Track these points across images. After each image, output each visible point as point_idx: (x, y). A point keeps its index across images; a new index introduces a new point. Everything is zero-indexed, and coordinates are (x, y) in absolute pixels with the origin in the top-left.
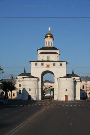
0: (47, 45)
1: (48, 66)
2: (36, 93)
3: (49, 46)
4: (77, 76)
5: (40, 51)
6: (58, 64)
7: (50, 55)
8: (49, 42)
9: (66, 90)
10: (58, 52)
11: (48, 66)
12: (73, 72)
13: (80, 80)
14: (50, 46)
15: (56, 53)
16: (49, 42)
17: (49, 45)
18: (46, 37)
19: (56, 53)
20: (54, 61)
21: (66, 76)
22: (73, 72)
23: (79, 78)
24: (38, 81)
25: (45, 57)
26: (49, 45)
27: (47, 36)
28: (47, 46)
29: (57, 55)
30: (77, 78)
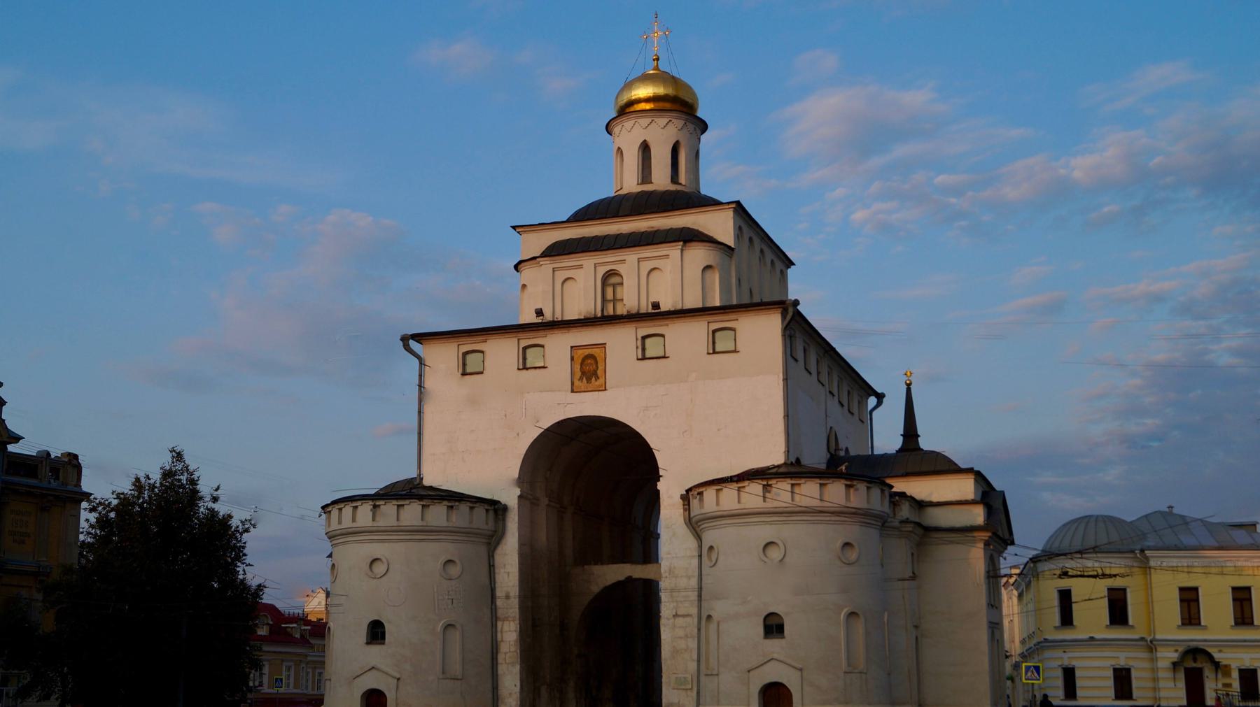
1: (589, 370)
2: (456, 669)
4: (941, 466)
6: (687, 338)
7: (628, 262)
8: (645, 148)
9: (773, 627)
11: (589, 370)
12: (910, 433)
13: (977, 515)
15: (689, 237)
16: (645, 148)
19: (689, 237)
22: (910, 433)
23: (964, 488)
24: (493, 539)
29: (698, 255)
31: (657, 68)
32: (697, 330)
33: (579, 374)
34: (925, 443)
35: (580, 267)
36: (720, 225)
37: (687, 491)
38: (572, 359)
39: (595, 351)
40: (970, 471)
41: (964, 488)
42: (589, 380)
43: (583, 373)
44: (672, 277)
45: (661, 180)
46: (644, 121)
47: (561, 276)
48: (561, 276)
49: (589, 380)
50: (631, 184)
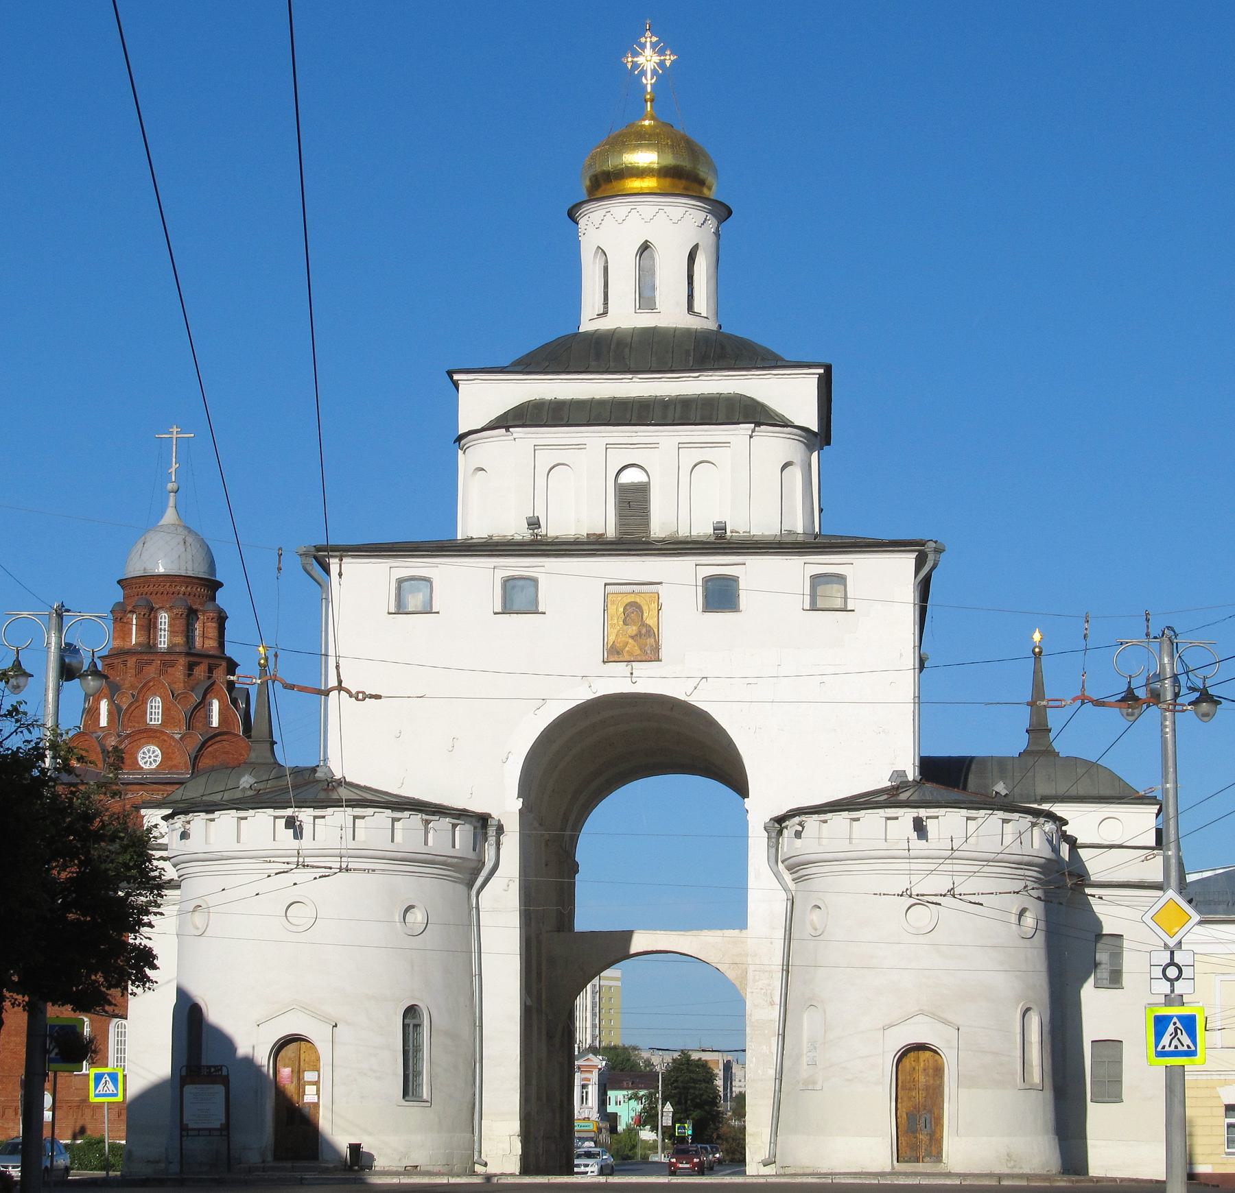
0: (609, 307)
3: (645, 321)
5: (482, 398)
6: (770, 582)
10: (794, 395)
14: (670, 313)
17: (646, 300)
18: (606, 184)
19: (753, 413)
20: (721, 543)
21: (911, 774)
25: (570, 479)
26: (646, 300)
27: (611, 164)
28: (624, 316)
29: (774, 447)
30: (1111, 835)
32: (795, 571)
35: (580, 447)
36: (794, 395)
44: (734, 478)
46: (648, 207)
47: (546, 459)
48: (546, 459)
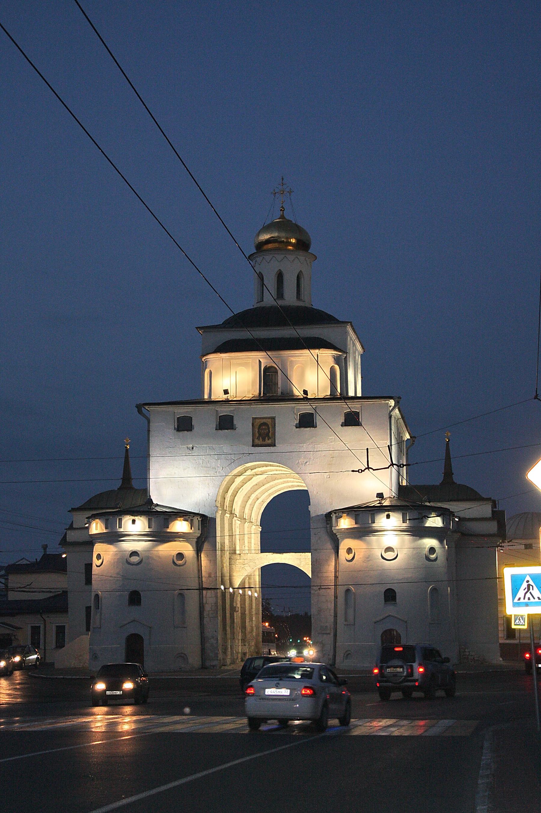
8: (280, 276)
12: (448, 473)
13: (492, 527)
16: (280, 276)
22: (448, 473)
23: (486, 510)
31: (282, 217)
33: (257, 435)
34: (458, 479)
37: (330, 513)
38: (253, 424)
39: (269, 421)
40: (489, 499)
41: (486, 510)
42: (264, 440)
43: (260, 435)
45: (290, 298)
49: (264, 440)
50: (269, 300)
